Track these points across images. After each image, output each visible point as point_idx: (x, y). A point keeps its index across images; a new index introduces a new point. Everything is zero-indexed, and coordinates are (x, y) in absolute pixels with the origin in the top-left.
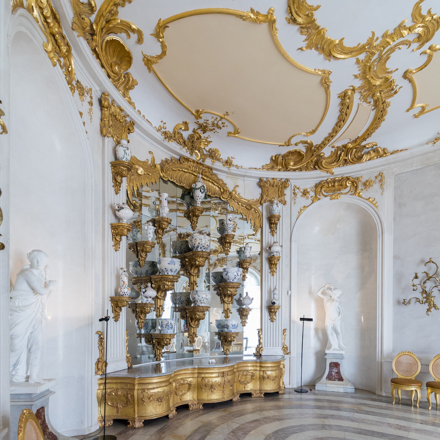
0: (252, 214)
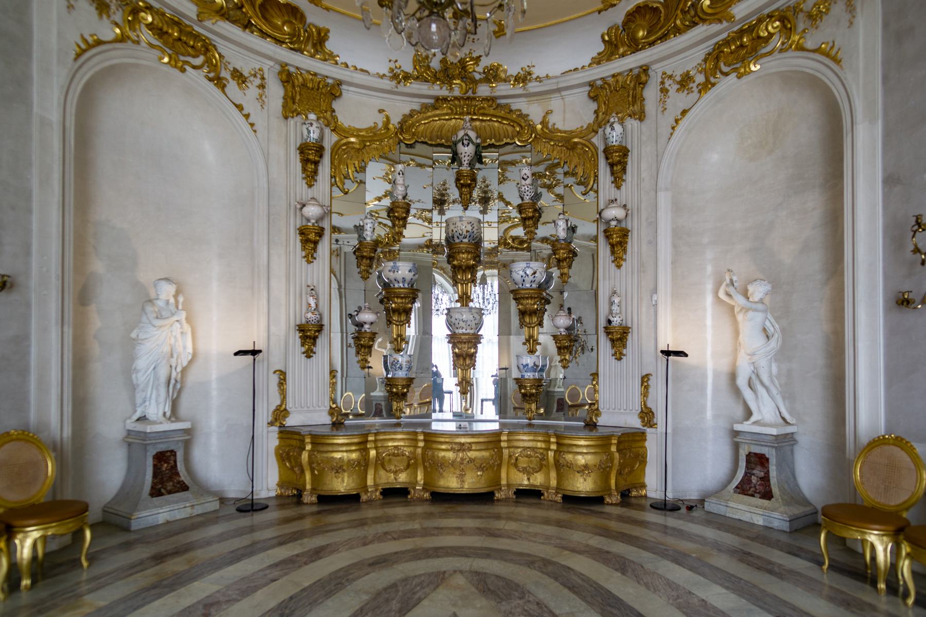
0: (579, 155)
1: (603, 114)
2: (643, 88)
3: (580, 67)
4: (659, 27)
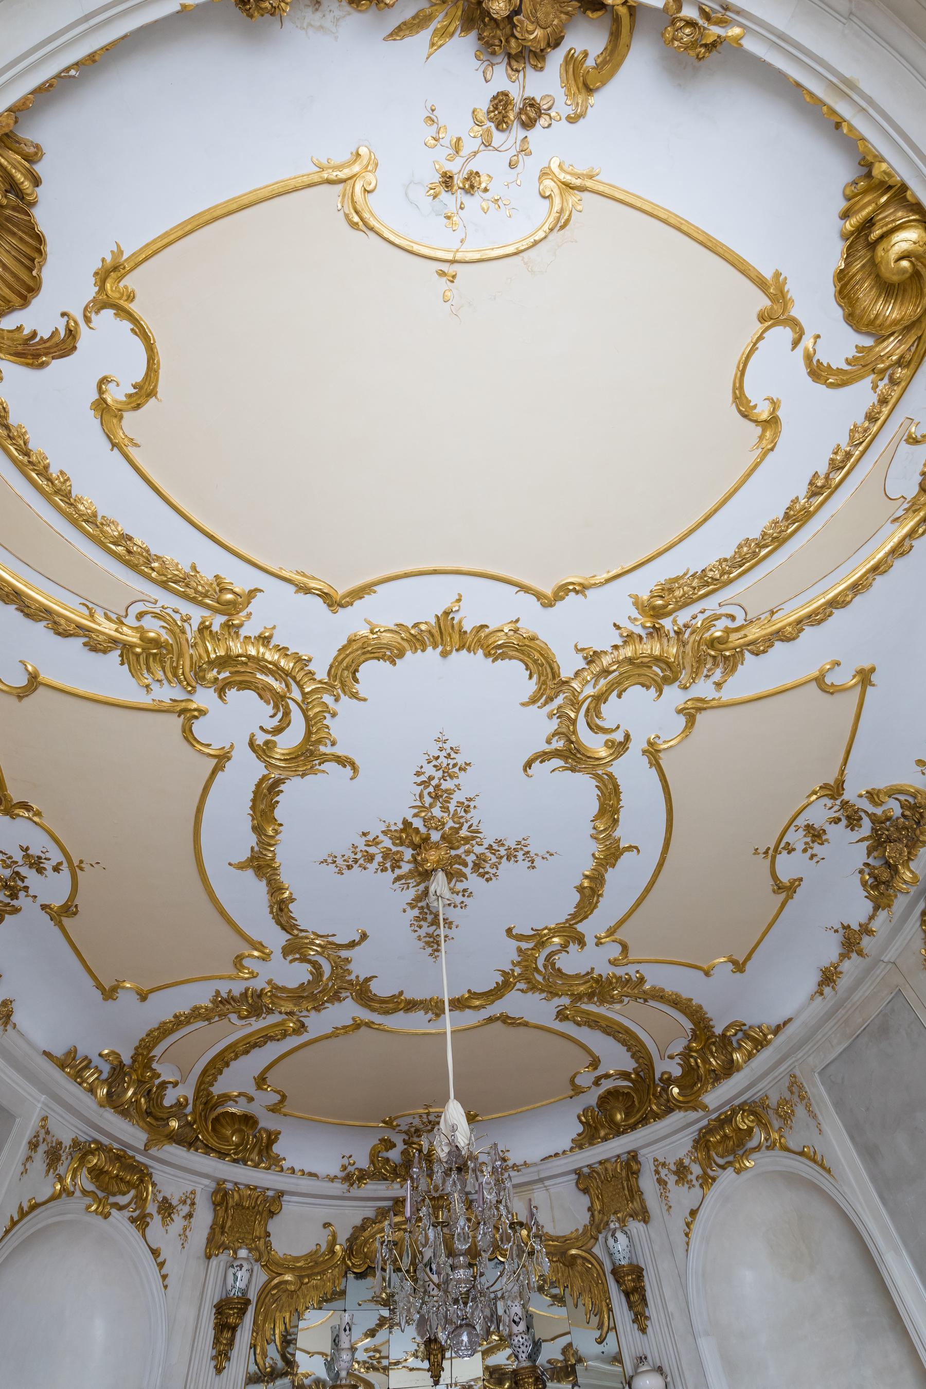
0: (581, 1274)
1: (599, 1212)
2: (637, 1179)
3: (560, 1152)
4: (635, 1110)
